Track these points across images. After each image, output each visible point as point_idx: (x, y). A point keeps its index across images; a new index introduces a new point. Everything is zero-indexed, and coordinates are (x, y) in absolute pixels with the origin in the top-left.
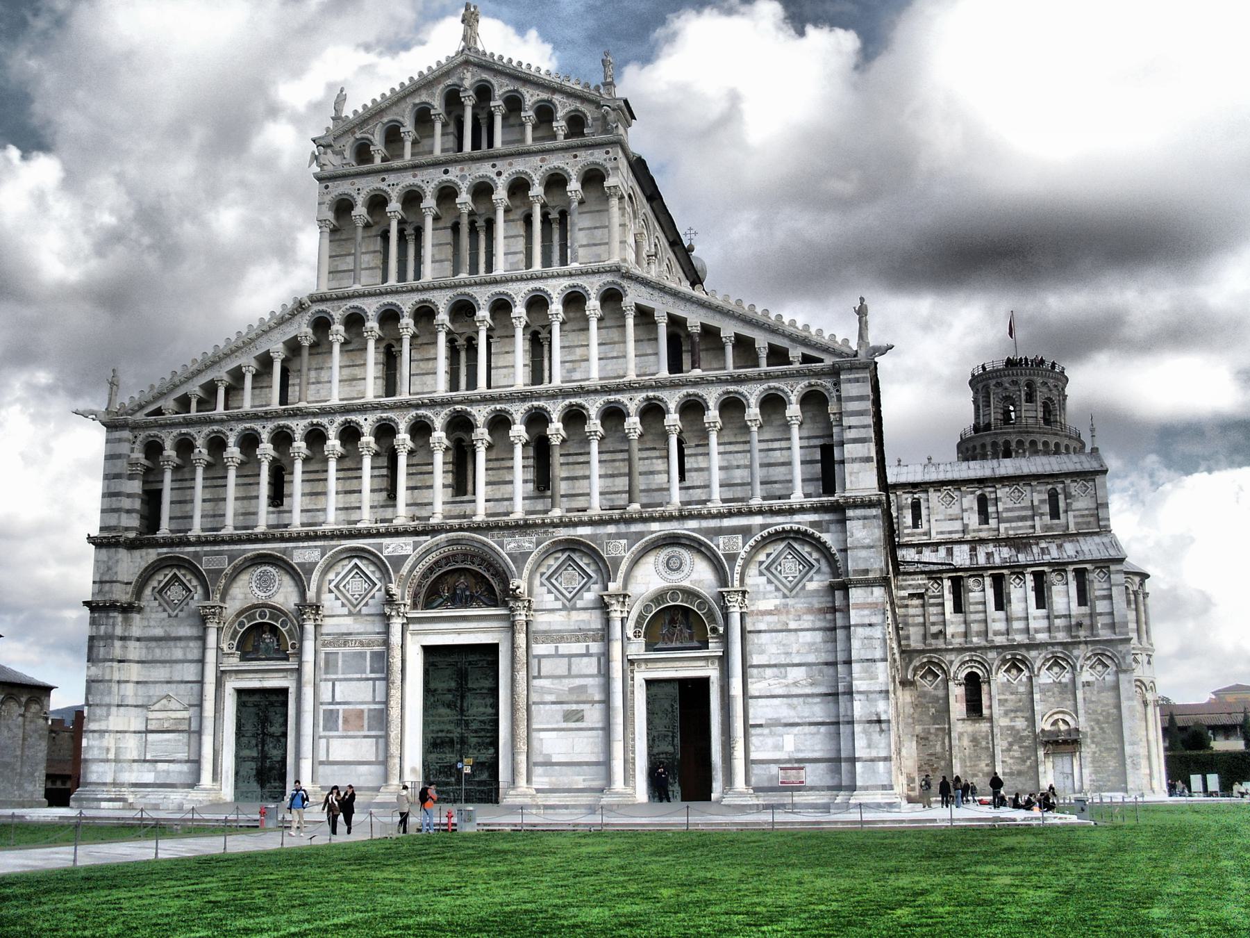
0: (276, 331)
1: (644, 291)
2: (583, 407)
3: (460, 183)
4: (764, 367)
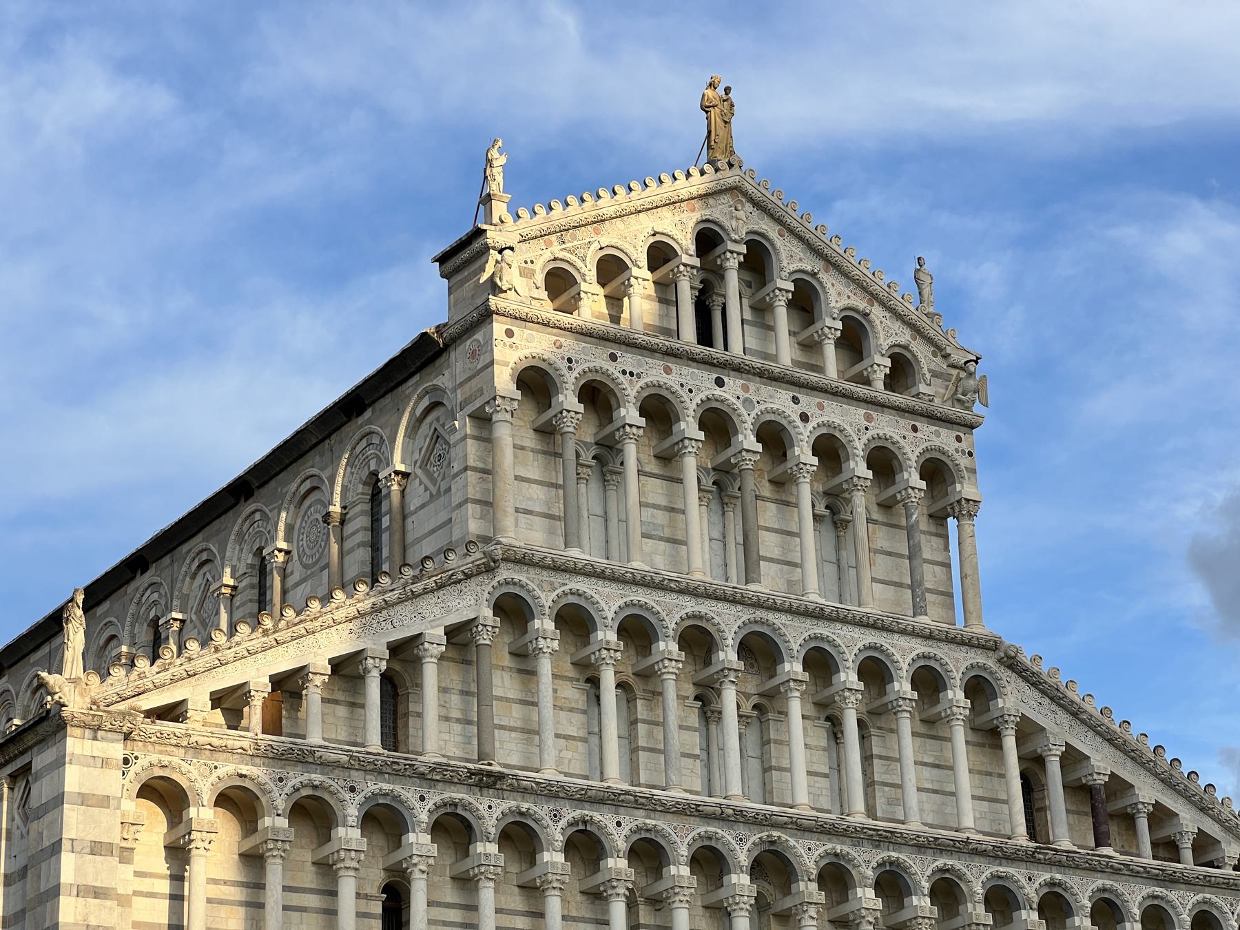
0: (432, 599)
1: (1032, 694)
2: (961, 876)
3: (743, 411)
4: (1187, 864)
